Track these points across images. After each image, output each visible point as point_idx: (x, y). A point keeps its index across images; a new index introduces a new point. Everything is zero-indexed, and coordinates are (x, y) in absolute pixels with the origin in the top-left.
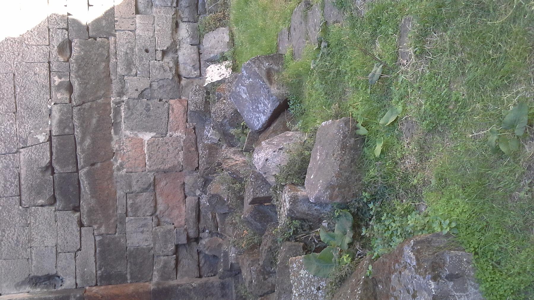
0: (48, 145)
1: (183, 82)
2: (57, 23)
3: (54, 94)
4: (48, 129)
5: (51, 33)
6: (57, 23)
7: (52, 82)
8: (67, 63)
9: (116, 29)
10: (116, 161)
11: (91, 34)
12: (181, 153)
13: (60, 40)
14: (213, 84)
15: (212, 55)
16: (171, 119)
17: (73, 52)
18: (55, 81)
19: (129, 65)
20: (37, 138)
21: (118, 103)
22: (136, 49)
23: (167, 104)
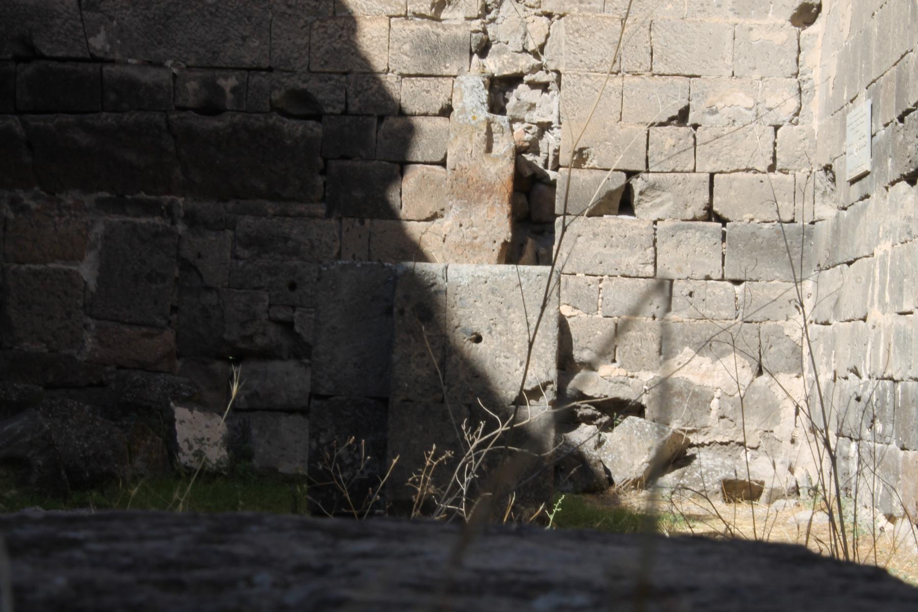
0: (81, 55)
1: (218, 366)
2: (360, 92)
3: (198, 74)
4: (118, 56)
5: (336, 77)
6: (360, 92)
7: (224, 73)
8: (268, 107)
9: (344, 220)
10: (36, 198)
11: (333, 164)
12: (42, 348)
13: (320, 97)
14: (171, 421)
15: (255, 432)
16: (127, 329)
17: (294, 122)
18: (226, 78)
19: (259, 243)
20: (99, 32)
21: (169, 212)
22: (295, 262)
23: (163, 322)
